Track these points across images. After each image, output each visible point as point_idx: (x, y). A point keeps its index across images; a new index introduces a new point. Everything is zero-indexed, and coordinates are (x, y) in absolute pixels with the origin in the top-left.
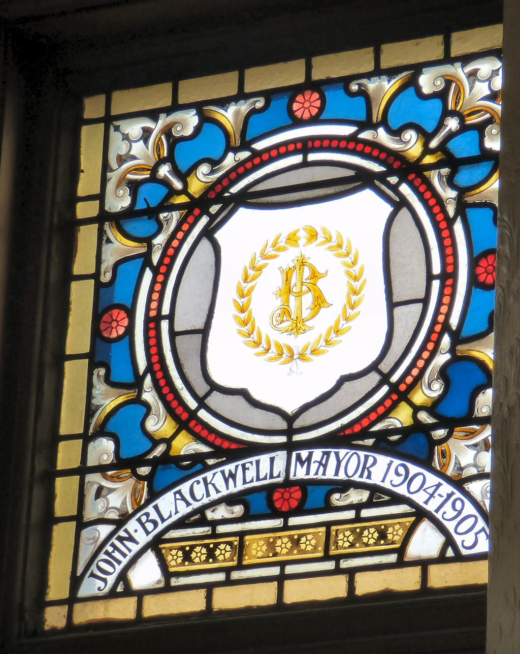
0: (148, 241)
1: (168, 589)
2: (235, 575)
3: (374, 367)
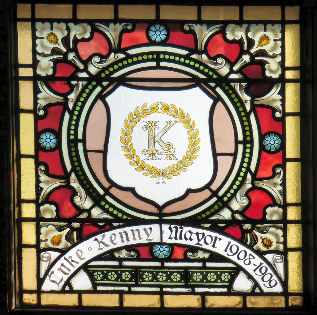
0: (65, 96)
1: (95, 291)
2: (134, 289)
3: (208, 186)
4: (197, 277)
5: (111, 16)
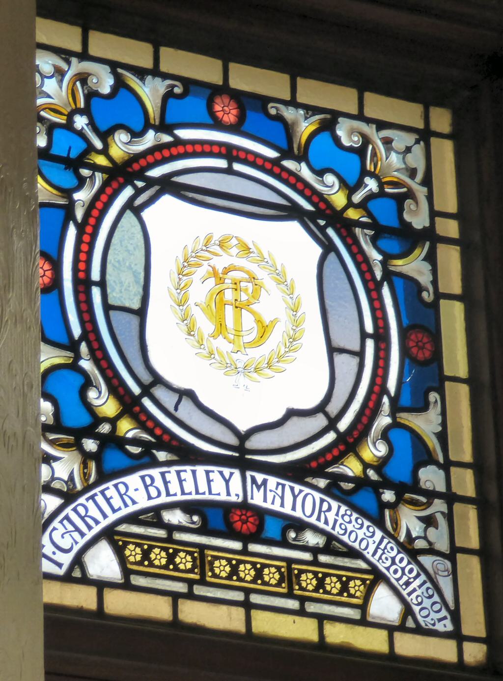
0: (67, 193)
1: (126, 586)
2: (198, 590)
3: (321, 408)
4: (308, 581)
5: (148, 64)
